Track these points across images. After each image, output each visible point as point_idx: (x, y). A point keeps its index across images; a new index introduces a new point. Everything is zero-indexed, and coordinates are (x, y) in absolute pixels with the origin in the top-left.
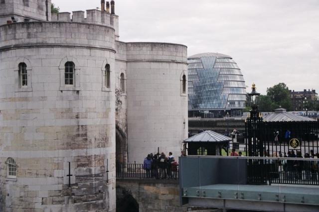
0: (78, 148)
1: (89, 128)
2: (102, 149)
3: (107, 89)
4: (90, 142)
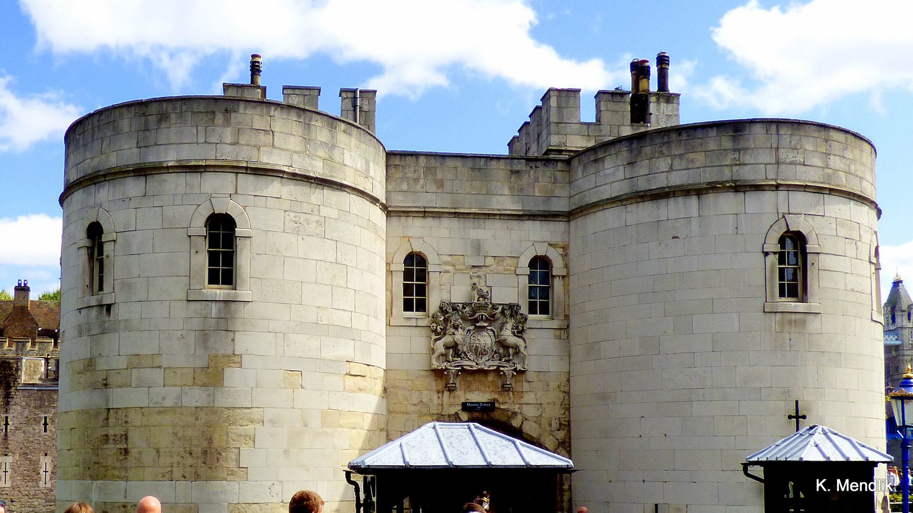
0: (104, 477)
2: (182, 485)
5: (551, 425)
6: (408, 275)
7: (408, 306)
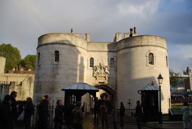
1: (42, 83)
3: (56, 63)
4: (42, 90)
5: (114, 86)
6: (91, 61)
7: (91, 66)
